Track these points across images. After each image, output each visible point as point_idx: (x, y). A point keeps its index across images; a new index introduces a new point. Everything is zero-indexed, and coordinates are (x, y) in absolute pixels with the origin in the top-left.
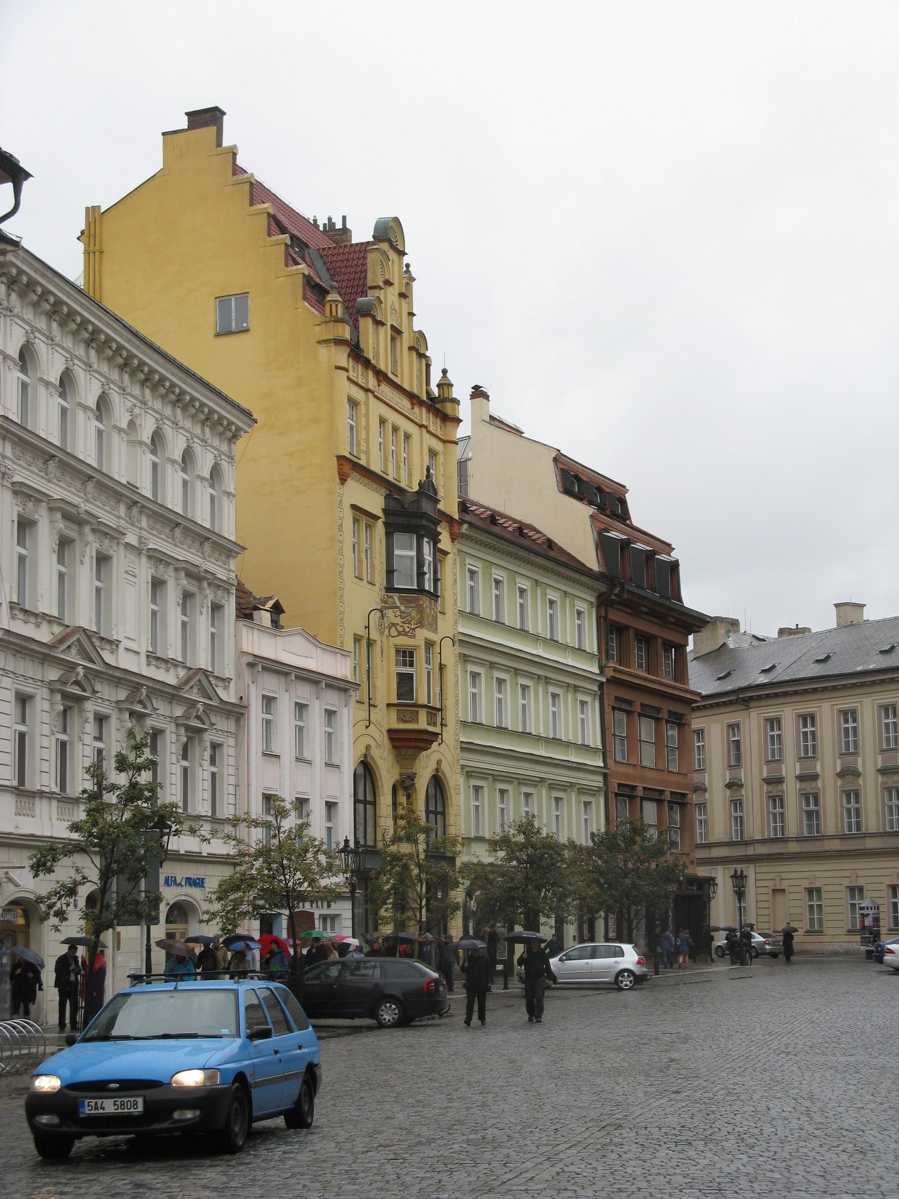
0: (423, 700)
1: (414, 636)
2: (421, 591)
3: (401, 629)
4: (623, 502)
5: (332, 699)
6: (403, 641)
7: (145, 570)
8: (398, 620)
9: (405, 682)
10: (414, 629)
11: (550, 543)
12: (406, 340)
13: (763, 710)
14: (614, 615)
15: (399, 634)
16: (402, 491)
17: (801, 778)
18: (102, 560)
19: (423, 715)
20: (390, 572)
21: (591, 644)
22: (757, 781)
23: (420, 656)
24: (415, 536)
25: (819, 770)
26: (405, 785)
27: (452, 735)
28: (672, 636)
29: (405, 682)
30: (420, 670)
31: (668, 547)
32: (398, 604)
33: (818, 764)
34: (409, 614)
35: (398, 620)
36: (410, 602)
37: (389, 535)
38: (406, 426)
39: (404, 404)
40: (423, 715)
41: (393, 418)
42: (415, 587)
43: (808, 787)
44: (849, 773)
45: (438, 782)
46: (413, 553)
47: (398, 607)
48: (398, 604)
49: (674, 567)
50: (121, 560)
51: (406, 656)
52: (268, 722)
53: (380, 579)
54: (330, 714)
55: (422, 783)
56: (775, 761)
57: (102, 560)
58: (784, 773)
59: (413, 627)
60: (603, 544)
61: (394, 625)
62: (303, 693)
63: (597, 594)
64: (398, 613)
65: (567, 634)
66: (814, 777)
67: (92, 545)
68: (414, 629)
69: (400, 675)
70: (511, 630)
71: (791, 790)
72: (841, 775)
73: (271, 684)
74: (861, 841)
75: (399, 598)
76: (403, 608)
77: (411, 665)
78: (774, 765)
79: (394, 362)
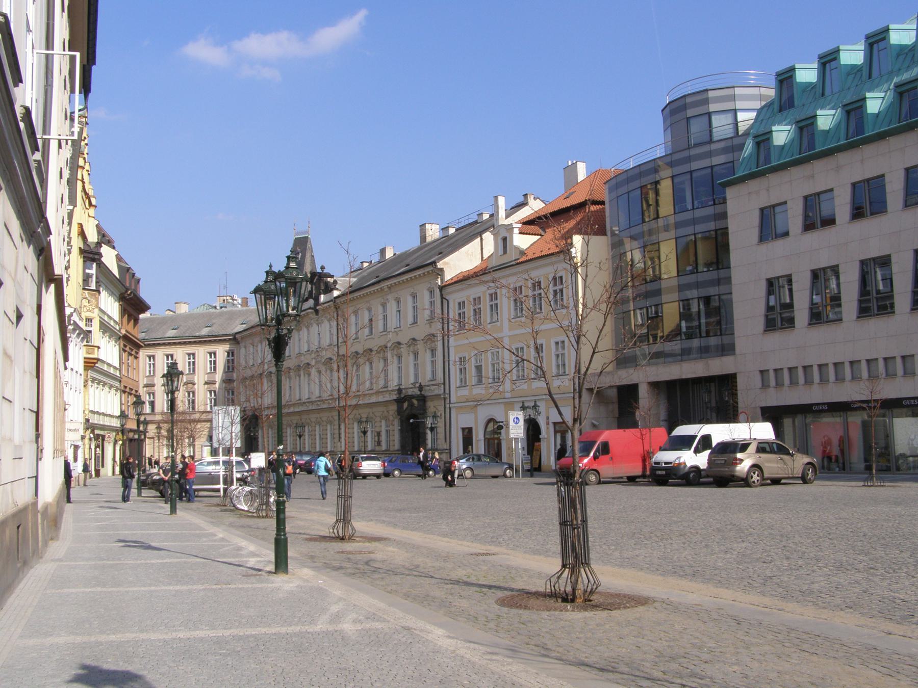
3: (88, 309)
13: (165, 350)
15: (88, 311)
24: (95, 264)
32: (87, 296)
48: (87, 296)
58: (156, 382)
61: (86, 306)
78: (151, 378)
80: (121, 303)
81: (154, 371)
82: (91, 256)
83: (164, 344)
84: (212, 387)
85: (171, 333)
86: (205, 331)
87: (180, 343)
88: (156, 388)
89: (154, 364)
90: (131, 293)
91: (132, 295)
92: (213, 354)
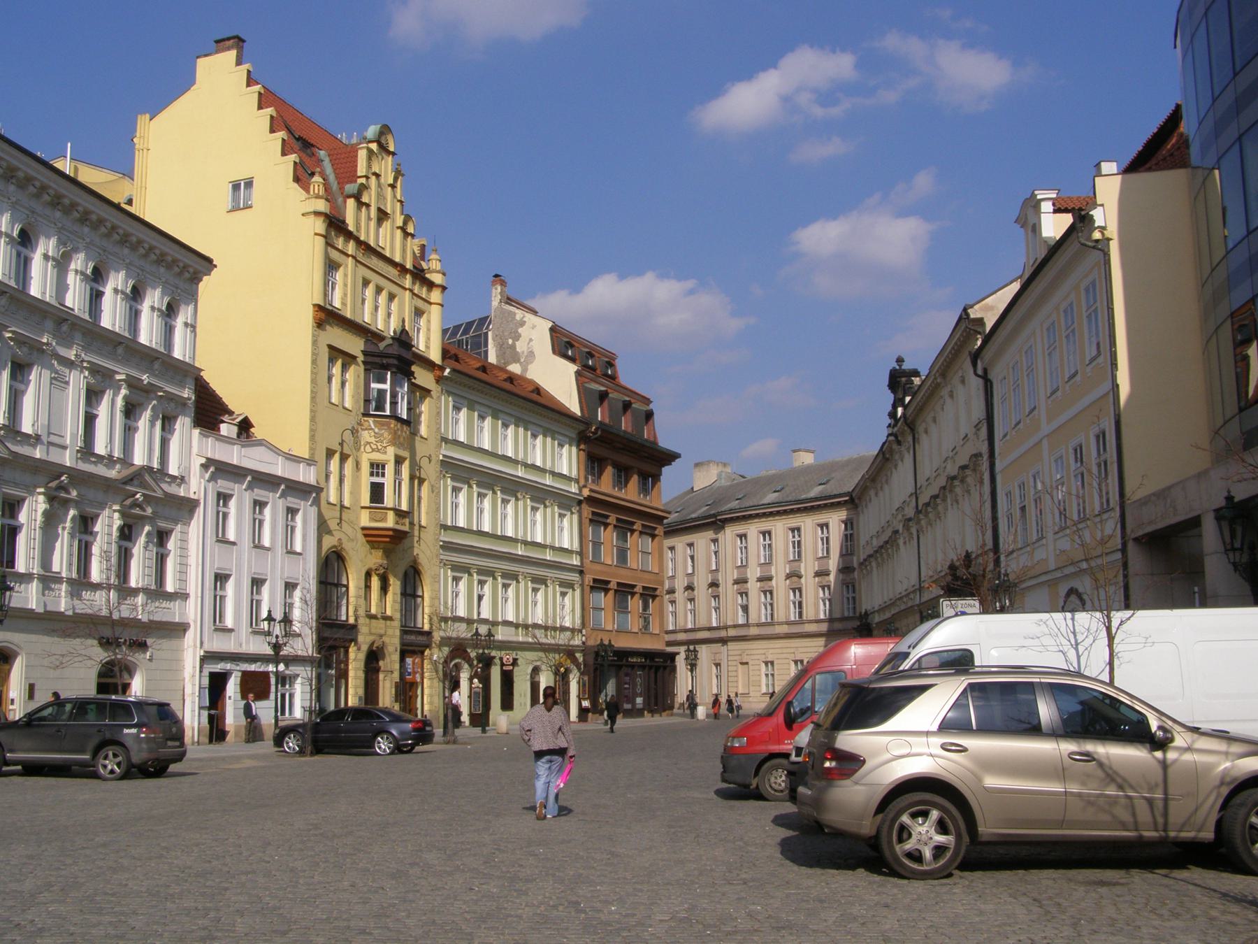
1: (385, 453)
3: (374, 447)
6: (377, 457)
8: (373, 440)
10: (385, 447)
15: (373, 450)
17: (760, 580)
22: (730, 582)
23: (390, 469)
25: (773, 573)
33: (773, 568)
34: (382, 435)
35: (373, 440)
36: (383, 425)
38: (395, 289)
39: (393, 272)
42: (388, 413)
43: (766, 585)
44: (794, 575)
46: (387, 386)
47: (372, 429)
59: (385, 445)
60: (583, 392)
61: (369, 443)
63: (577, 432)
64: (373, 434)
66: (770, 579)
68: (385, 447)
69: (372, 484)
71: (753, 587)
72: (788, 577)
74: (802, 626)
75: (374, 422)
76: (376, 430)
77: (383, 475)
78: (742, 569)
80: (582, 447)
81: (747, 558)
82: (377, 360)
83: (757, 516)
84: (825, 580)
85: (771, 497)
86: (815, 491)
87: (778, 513)
88: (749, 584)
89: (746, 548)
90: (597, 429)
91: (599, 433)
92: (824, 526)
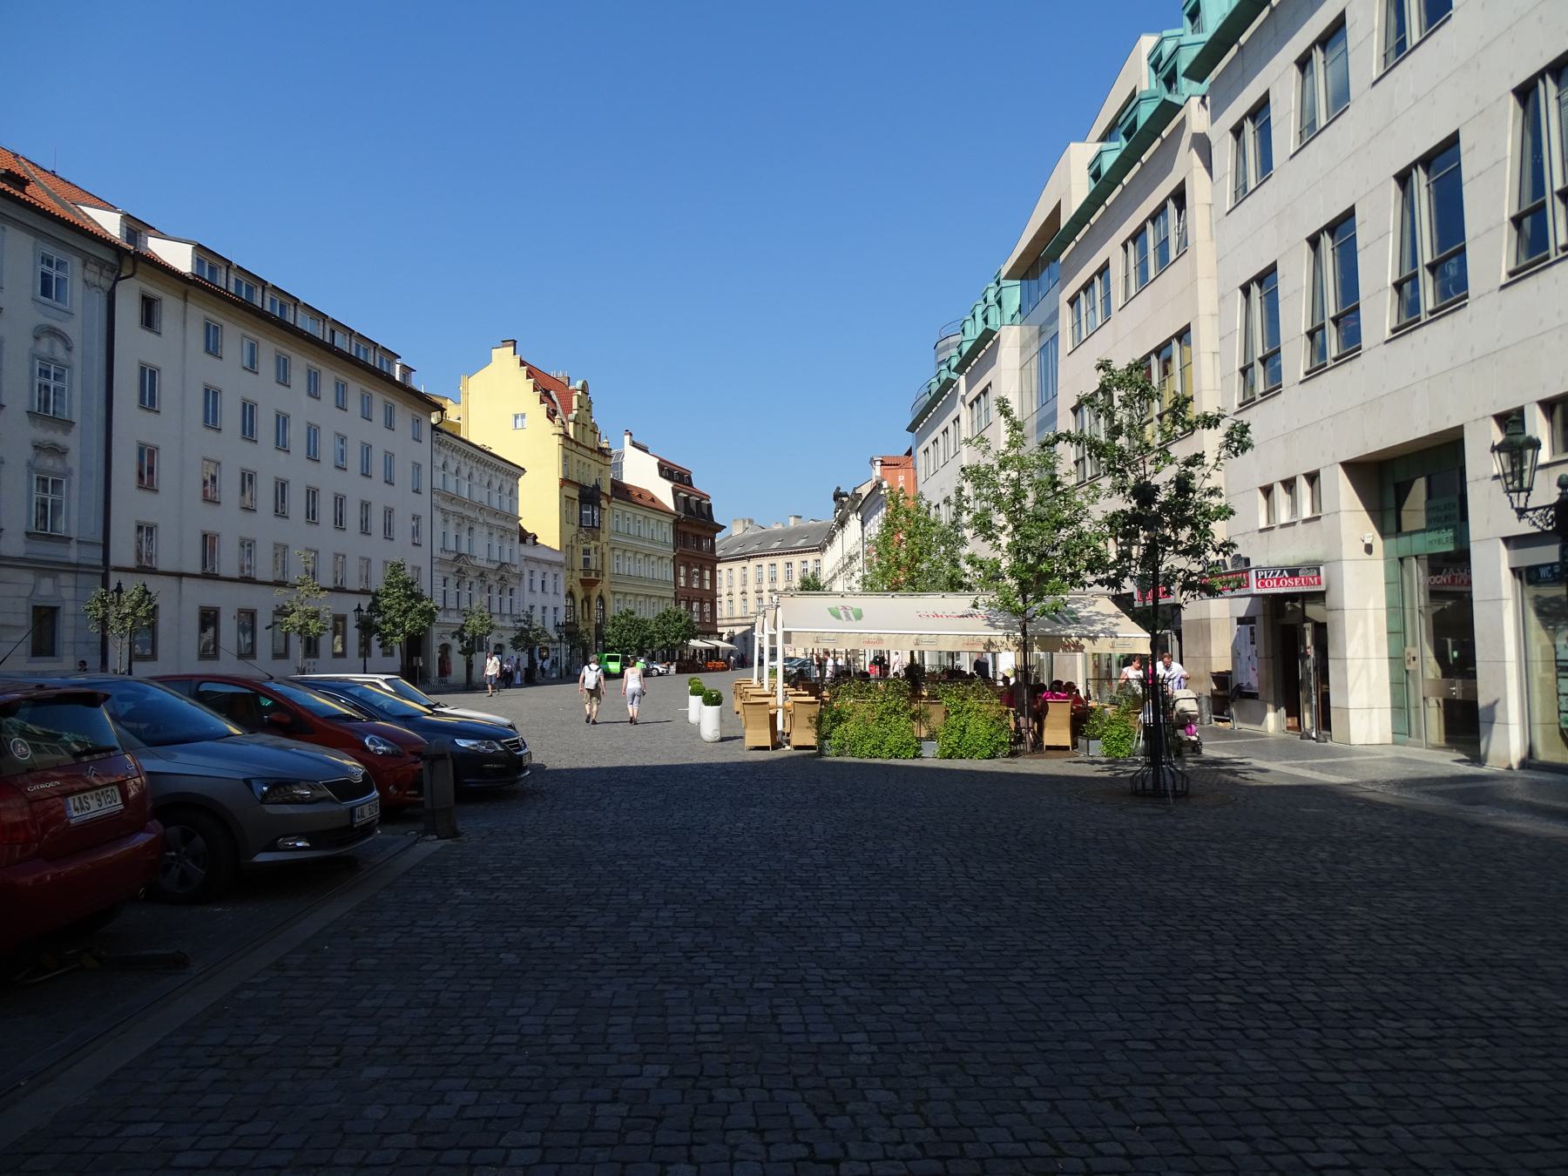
0: (593, 568)
2: (593, 526)
4: (689, 478)
5: (556, 570)
6: (586, 546)
7: (485, 530)
9: (586, 561)
11: (653, 500)
12: (590, 427)
14: (680, 528)
16: (586, 487)
17: (770, 591)
18: (470, 529)
19: (593, 574)
20: (581, 519)
21: (670, 539)
23: (592, 551)
26: (587, 599)
27: (606, 579)
28: (708, 534)
29: (586, 561)
30: (592, 557)
31: (707, 498)
37: (580, 505)
40: (593, 574)
41: (586, 460)
45: (601, 598)
49: (710, 506)
50: (477, 528)
51: (586, 552)
52: (531, 580)
53: (577, 522)
54: (556, 575)
55: (594, 598)
56: (760, 581)
57: (470, 529)
62: (545, 568)
65: (658, 536)
67: (467, 525)
70: (634, 538)
73: (533, 566)
79: (583, 437)
